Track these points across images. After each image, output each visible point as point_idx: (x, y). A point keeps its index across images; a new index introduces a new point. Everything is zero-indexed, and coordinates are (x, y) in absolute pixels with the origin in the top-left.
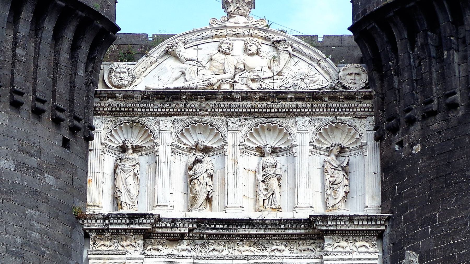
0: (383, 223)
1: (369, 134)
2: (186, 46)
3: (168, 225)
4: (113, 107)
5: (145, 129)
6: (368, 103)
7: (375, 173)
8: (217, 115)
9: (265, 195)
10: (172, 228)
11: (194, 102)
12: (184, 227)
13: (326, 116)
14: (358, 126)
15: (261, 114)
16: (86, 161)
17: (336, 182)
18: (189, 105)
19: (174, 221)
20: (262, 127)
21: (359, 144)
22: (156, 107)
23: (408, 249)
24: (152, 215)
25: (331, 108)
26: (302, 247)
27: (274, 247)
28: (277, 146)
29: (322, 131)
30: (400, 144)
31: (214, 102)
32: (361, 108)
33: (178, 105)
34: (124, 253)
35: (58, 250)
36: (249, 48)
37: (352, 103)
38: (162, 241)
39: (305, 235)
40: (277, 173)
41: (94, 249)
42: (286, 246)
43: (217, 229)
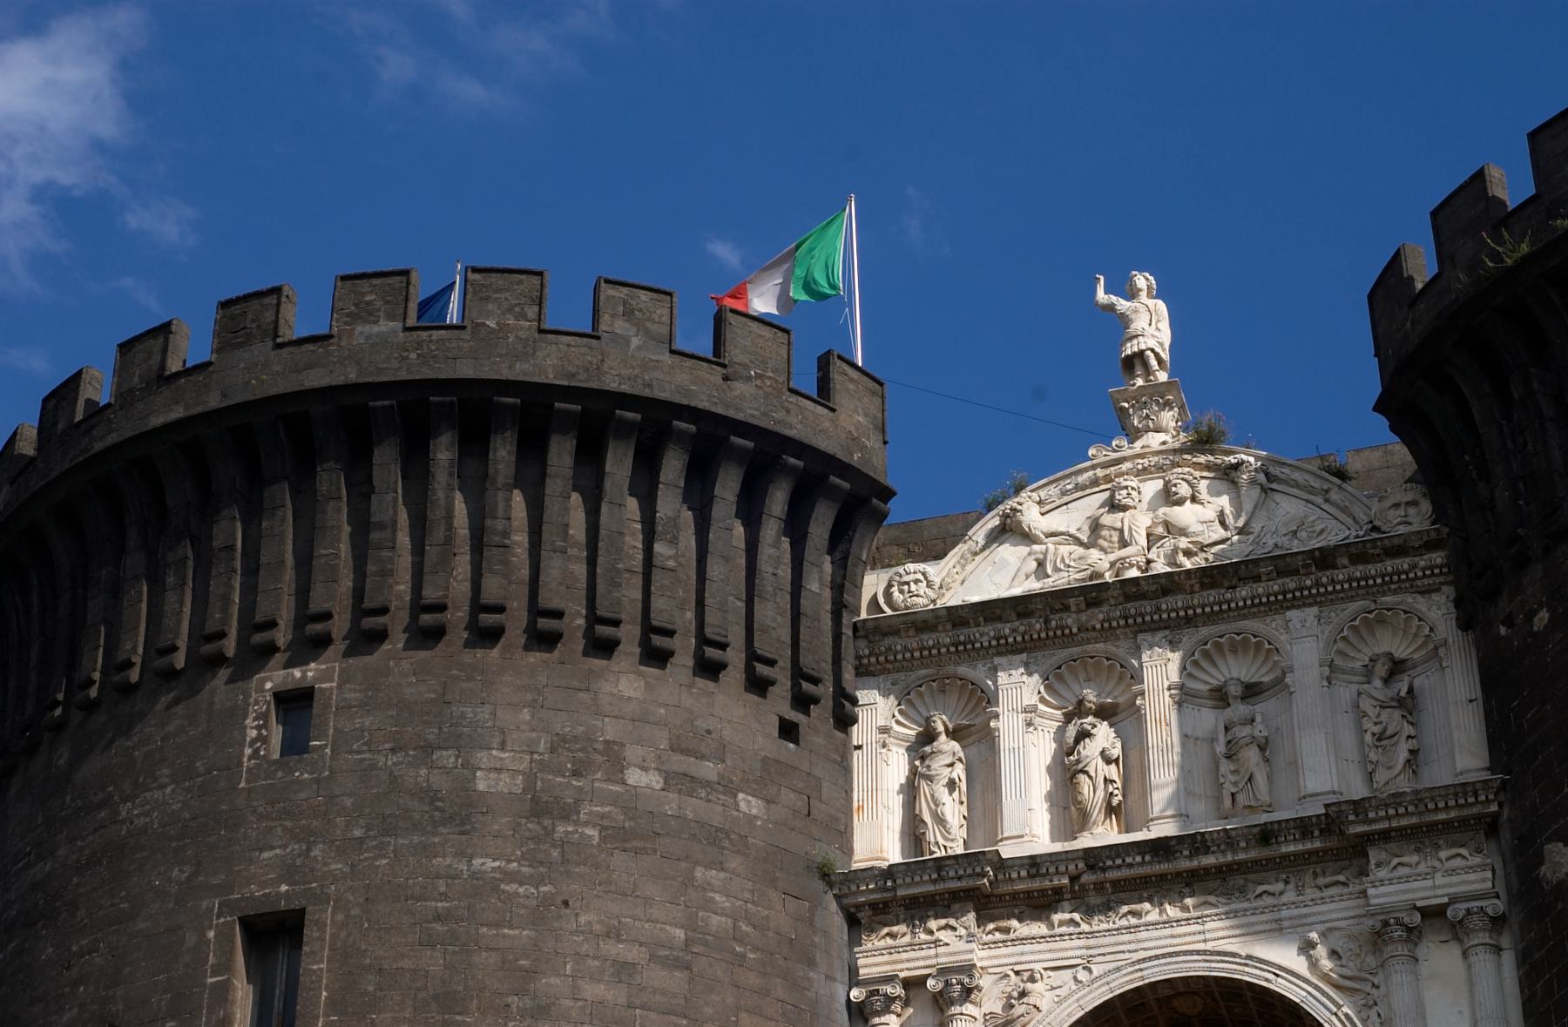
0: (1491, 797)
1: (1449, 622)
2: (1044, 510)
3: (1024, 873)
5: (970, 687)
6: (1438, 557)
7: (1471, 701)
8: (1116, 635)
9: (1235, 784)
10: (1031, 876)
11: (1064, 616)
13: (1352, 599)
14: (1424, 609)
15: (1212, 618)
16: (847, 771)
17: (1388, 733)
20: (1218, 646)
21: (1431, 646)
22: (986, 638)
23: (1549, 840)
25: (1358, 580)
26: (1321, 881)
27: (1260, 889)
28: (1254, 680)
29: (1345, 633)
30: (1509, 621)
31: (1105, 608)
32: (1423, 570)
33: (1030, 626)
34: (933, 946)
35: (778, 950)
36: (1174, 489)
37: (1404, 563)
38: (1016, 911)
39: (1325, 851)
40: (1257, 733)
41: (869, 945)
42: (1287, 882)
43: (1131, 865)
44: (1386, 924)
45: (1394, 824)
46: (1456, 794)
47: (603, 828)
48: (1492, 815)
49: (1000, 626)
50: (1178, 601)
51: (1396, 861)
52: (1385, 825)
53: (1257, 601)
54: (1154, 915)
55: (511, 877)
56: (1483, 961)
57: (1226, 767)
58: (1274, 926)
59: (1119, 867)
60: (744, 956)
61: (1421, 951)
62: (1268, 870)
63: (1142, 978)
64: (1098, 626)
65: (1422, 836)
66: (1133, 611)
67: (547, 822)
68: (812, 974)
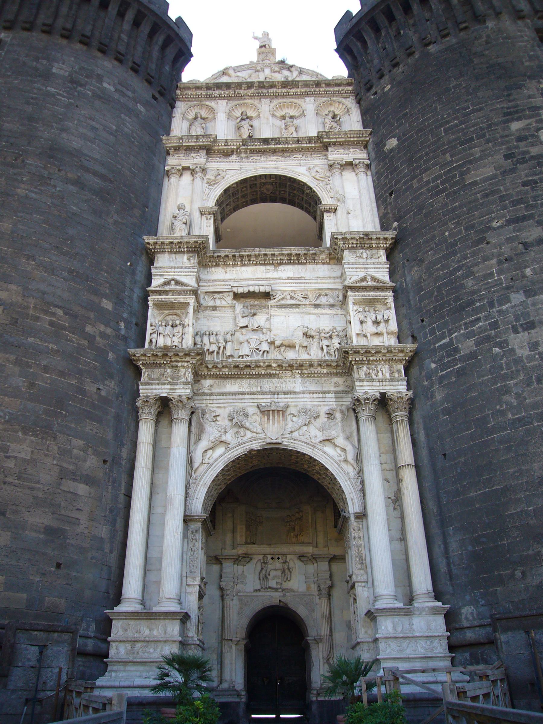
3: (223, 144)
6: (350, 88)
10: (226, 146)
12: (233, 145)
13: (324, 97)
19: (226, 141)
24: (211, 135)
27: (294, 156)
31: (253, 90)
33: (230, 92)
39: (315, 147)
44: (334, 163)
45: (338, 140)
46: (357, 134)
47: (93, 93)
48: (366, 141)
49: (220, 91)
50: (274, 90)
54: (262, 159)
55: (60, 95)
56: (362, 176)
57: (284, 131)
60: (134, 142)
61: (343, 173)
65: (345, 144)
67: (75, 86)
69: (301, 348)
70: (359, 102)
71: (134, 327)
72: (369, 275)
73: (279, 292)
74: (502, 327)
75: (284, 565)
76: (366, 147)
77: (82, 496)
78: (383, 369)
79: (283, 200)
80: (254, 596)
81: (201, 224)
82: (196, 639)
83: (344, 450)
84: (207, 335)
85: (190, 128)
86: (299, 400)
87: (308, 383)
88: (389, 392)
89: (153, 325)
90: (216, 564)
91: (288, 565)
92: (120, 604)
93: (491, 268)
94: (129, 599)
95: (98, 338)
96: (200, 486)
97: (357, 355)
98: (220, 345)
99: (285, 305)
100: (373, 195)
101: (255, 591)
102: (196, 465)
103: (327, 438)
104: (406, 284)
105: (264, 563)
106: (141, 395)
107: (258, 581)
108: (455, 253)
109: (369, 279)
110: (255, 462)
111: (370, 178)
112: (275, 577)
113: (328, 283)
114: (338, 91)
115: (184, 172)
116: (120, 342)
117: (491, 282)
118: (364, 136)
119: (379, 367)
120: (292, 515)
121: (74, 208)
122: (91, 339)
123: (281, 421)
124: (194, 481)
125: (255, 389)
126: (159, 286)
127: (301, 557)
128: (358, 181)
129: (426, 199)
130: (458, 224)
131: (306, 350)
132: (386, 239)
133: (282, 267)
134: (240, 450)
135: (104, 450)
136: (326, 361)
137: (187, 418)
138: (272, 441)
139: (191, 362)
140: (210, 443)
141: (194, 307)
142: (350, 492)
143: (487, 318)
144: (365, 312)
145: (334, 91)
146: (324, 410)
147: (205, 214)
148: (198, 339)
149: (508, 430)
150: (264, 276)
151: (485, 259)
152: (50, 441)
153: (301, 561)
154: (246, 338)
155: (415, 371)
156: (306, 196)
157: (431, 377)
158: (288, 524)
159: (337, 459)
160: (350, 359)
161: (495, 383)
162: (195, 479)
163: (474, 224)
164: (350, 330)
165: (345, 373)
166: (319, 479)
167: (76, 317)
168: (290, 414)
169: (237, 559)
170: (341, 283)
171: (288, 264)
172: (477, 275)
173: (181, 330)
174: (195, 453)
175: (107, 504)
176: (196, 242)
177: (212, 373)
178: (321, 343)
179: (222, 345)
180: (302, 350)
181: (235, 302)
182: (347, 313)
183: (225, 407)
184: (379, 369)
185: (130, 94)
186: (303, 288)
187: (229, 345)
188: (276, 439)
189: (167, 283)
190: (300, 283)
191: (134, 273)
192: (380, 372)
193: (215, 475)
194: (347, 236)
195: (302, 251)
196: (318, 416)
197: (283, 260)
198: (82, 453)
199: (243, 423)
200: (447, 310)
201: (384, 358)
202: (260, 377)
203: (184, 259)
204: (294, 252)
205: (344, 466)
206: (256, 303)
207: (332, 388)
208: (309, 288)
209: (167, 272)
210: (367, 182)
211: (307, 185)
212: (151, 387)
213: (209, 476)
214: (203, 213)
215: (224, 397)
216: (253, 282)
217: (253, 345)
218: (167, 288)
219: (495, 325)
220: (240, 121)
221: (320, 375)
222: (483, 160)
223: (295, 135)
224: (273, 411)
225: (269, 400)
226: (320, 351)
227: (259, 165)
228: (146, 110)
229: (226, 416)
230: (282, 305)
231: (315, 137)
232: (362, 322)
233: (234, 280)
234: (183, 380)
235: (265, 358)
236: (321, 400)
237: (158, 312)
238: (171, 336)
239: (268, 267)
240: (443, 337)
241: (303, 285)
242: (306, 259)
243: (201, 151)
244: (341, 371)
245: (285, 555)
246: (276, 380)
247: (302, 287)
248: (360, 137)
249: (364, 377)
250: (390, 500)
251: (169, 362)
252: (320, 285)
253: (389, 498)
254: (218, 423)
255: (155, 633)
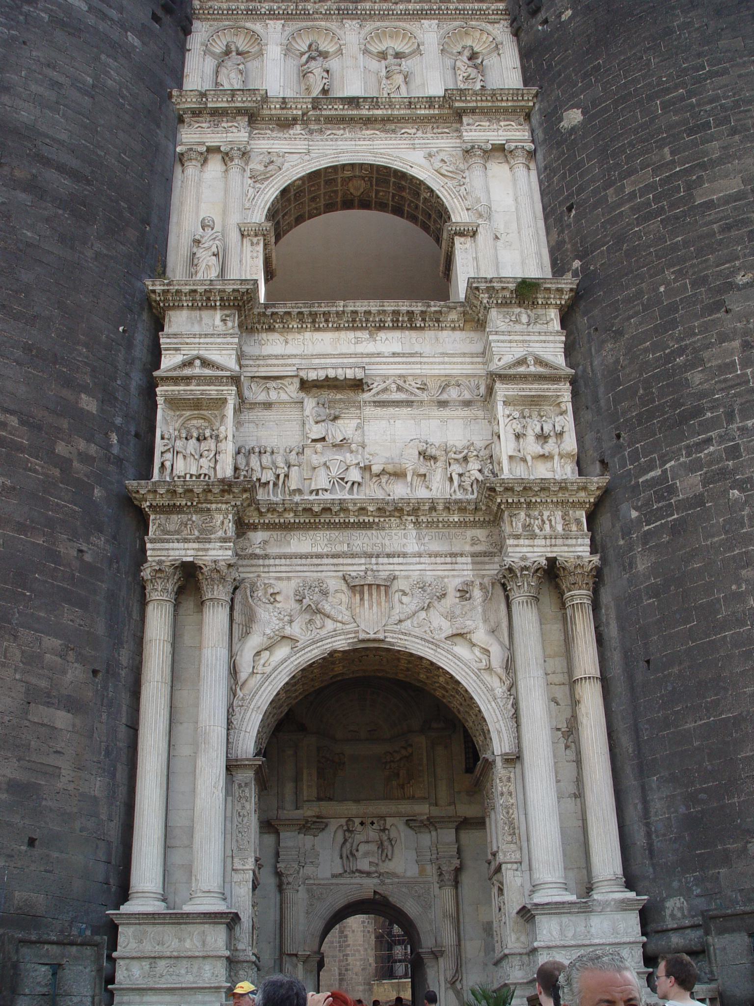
0: (530, 98)
3: (278, 106)
4: (215, 10)
12: (296, 108)
13: (455, 19)
14: (491, 29)
17: (471, 77)
18: (300, 7)
25: (460, 10)
27: (403, 131)
28: (401, 51)
32: (493, 10)
38: (271, 127)
39: (440, 116)
42: (418, 130)
44: (473, 147)
45: (479, 104)
46: (513, 94)
49: (272, 4)
51: (477, 124)
52: (473, 104)
53: (407, 12)
54: (347, 135)
56: (521, 171)
57: (384, 81)
58: (411, 146)
59: (330, 109)
61: (488, 165)
62: (408, 123)
63: (338, 161)
64: (324, 12)
66: (343, 7)
68: (158, 131)
69: (415, 478)
70: (516, 34)
71: (133, 441)
72: (530, 354)
73: (378, 378)
74: (745, 456)
75: (381, 834)
76: (528, 117)
77: (61, 730)
78: (553, 518)
79: (382, 206)
80: (332, 884)
81: (242, 252)
82: (251, 954)
83: (486, 652)
84: (257, 454)
85: (217, 72)
86: (412, 567)
87: (427, 539)
88: (561, 556)
89: (166, 436)
90: (269, 833)
91: (389, 835)
92: (128, 900)
93: (732, 354)
94: (143, 892)
95: (75, 464)
96: (250, 711)
97: (510, 493)
98: (279, 471)
99: (388, 402)
100: (539, 207)
101: (334, 876)
102: (243, 676)
103: (459, 632)
104: (593, 371)
105: (348, 830)
106: (149, 558)
107: (338, 860)
108: (674, 324)
109: (531, 361)
110: (338, 669)
111: (534, 173)
112: (366, 854)
113: (461, 363)
114: (480, 10)
115: (210, 156)
116: (112, 468)
117: (731, 379)
118: (526, 98)
119: (546, 514)
120: (395, 752)
121: (29, 234)
122: (64, 464)
123: (383, 603)
124: (240, 703)
125: (339, 548)
126: (174, 369)
127: (411, 822)
128: (515, 181)
129: (628, 224)
130: (680, 274)
131: (424, 481)
132: (560, 291)
133: (382, 335)
134: (316, 651)
135: (93, 653)
136: (457, 502)
137: (228, 599)
138: (368, 636)
139: (233, 503)
140: (265, 639)
141: (235, 405)
142: (496, 720)
143: (722, 439)
144: (524, 417)
145: (472, 10)
146: (453, 583)
147: (249, 235)
148: (241, 461)
149: (748, 625)
150: (351, 349)
151: (723, 338)
152: (8, 641)
153: (410, 827)
154: (323, 460)
155: (605, 521)
156: (424, 203)
157: (630, 533)
158: (388, 767)
159: (475, 666)
160: (499, 501)
161: (731, 549)
162: (243, 699)
163: (707, 276)
164: (498, 448)
165: (489, 522)
166: (444, 696)
167: (40, 428)
168: (396, 591)
169: (304, 826)
170: (484, 364)
171: (394, 328)
172: (710, 365)
173: (213, 447)
174: (241, 656)
175: (101, 742)
176: (238, 291)
177: (267, 521)
178: (450, 470)
179: (282, 472)
180: (417, 481)
181: (302, 395)
182: (492, 419)
183: (289, 578)
184: (545, 518)
185: (113, 14)
186: (419, 371)
187: (294, 471)
188: (375, 633)
189: (188, 363)
190: (413, 363)
191: (130, 346)
192: (547, 522)
193: (275, 693)
194: (495, 285)
195: (418, 307)
196: (444, 595)
197: (385, 322)
198: (58, 659)
199: (319, 606)
200: (658, 422)
201: (555, 500)
202: (347, 527)
203: (215, 319)
204: (404, 309)
205: (486, 677)
206: (339, 396)
207: (468, 548)
208: (428, 371)
209: (187, 344)
210: (530, 183)
211: (425, 184)
212: (166, 545)
213: (265, 695)
214: (246, 233)
215: (288, 562)
216: (334, 361)
217: (335, 472)
218: (187, 372)
219: (734, 452)
220: (307, 62)
221: (448, 525)
222: (725, 164)
223: (404, 92)
224: (370, 585)
225: (363, 568)
226: (448, 483)
227: (342, 145)
228: (144, 43)
229: (292, 594)
230: (384, 402)
231: (439, 97)
232: (518, 436)
233: (302, 357)
234: (220, 533)
235: (355, 497)
236: (449, 567)
237: (173, 413)
238: (196, 457)
239: (359, 334)
240: (651, 467)
241: (419, 366)
242: (424, 320)
243: (239, 118)
244: (482, 519)
245: (382, 818)
246: (374, 532)
247: (416, 370)
248: (518, 100)
249: (521, 530)
250: (560, 733)
251: (195, 504)
252: (447, 366)
253: (558, 729)
254: (278, 605)
255: (188, 944)
